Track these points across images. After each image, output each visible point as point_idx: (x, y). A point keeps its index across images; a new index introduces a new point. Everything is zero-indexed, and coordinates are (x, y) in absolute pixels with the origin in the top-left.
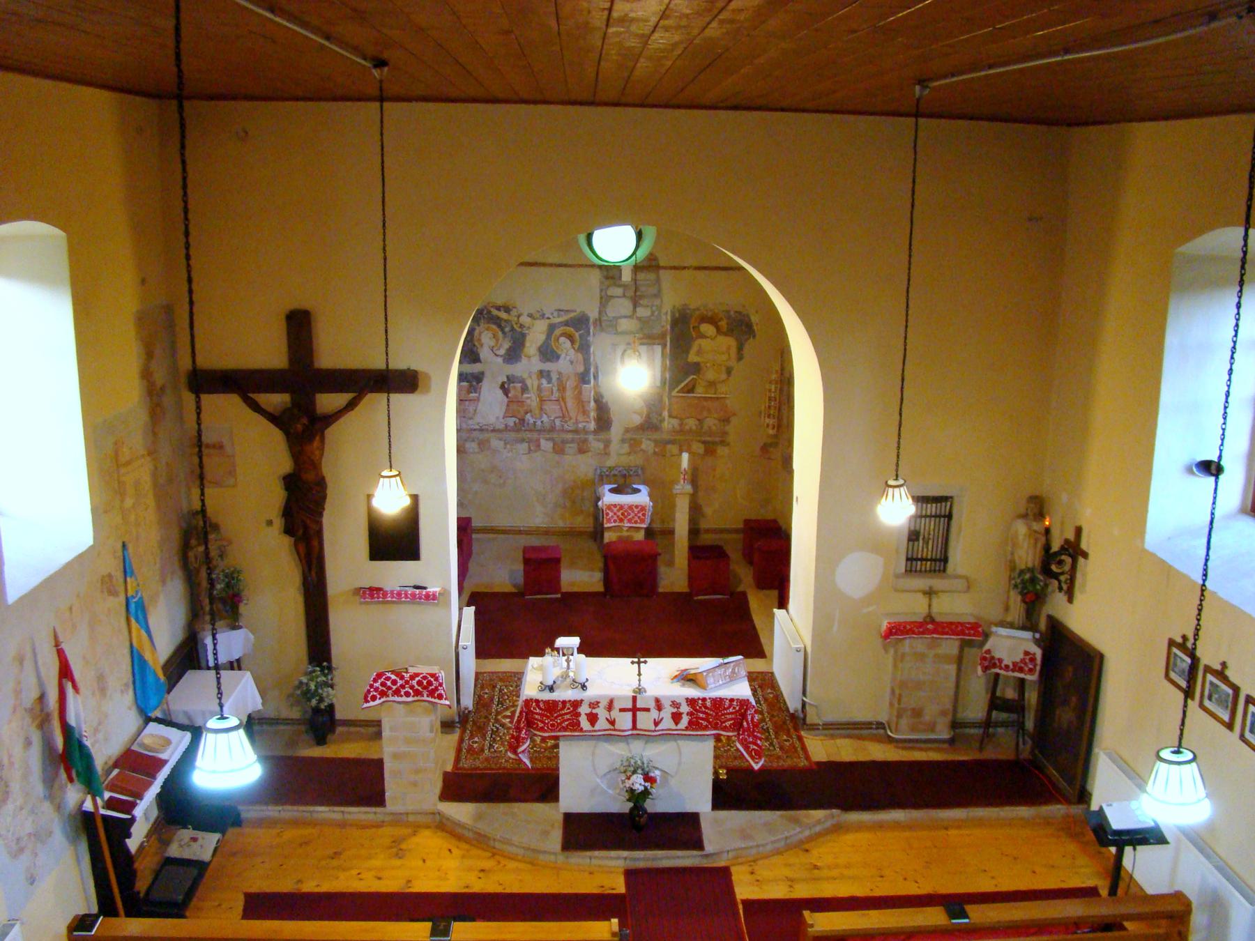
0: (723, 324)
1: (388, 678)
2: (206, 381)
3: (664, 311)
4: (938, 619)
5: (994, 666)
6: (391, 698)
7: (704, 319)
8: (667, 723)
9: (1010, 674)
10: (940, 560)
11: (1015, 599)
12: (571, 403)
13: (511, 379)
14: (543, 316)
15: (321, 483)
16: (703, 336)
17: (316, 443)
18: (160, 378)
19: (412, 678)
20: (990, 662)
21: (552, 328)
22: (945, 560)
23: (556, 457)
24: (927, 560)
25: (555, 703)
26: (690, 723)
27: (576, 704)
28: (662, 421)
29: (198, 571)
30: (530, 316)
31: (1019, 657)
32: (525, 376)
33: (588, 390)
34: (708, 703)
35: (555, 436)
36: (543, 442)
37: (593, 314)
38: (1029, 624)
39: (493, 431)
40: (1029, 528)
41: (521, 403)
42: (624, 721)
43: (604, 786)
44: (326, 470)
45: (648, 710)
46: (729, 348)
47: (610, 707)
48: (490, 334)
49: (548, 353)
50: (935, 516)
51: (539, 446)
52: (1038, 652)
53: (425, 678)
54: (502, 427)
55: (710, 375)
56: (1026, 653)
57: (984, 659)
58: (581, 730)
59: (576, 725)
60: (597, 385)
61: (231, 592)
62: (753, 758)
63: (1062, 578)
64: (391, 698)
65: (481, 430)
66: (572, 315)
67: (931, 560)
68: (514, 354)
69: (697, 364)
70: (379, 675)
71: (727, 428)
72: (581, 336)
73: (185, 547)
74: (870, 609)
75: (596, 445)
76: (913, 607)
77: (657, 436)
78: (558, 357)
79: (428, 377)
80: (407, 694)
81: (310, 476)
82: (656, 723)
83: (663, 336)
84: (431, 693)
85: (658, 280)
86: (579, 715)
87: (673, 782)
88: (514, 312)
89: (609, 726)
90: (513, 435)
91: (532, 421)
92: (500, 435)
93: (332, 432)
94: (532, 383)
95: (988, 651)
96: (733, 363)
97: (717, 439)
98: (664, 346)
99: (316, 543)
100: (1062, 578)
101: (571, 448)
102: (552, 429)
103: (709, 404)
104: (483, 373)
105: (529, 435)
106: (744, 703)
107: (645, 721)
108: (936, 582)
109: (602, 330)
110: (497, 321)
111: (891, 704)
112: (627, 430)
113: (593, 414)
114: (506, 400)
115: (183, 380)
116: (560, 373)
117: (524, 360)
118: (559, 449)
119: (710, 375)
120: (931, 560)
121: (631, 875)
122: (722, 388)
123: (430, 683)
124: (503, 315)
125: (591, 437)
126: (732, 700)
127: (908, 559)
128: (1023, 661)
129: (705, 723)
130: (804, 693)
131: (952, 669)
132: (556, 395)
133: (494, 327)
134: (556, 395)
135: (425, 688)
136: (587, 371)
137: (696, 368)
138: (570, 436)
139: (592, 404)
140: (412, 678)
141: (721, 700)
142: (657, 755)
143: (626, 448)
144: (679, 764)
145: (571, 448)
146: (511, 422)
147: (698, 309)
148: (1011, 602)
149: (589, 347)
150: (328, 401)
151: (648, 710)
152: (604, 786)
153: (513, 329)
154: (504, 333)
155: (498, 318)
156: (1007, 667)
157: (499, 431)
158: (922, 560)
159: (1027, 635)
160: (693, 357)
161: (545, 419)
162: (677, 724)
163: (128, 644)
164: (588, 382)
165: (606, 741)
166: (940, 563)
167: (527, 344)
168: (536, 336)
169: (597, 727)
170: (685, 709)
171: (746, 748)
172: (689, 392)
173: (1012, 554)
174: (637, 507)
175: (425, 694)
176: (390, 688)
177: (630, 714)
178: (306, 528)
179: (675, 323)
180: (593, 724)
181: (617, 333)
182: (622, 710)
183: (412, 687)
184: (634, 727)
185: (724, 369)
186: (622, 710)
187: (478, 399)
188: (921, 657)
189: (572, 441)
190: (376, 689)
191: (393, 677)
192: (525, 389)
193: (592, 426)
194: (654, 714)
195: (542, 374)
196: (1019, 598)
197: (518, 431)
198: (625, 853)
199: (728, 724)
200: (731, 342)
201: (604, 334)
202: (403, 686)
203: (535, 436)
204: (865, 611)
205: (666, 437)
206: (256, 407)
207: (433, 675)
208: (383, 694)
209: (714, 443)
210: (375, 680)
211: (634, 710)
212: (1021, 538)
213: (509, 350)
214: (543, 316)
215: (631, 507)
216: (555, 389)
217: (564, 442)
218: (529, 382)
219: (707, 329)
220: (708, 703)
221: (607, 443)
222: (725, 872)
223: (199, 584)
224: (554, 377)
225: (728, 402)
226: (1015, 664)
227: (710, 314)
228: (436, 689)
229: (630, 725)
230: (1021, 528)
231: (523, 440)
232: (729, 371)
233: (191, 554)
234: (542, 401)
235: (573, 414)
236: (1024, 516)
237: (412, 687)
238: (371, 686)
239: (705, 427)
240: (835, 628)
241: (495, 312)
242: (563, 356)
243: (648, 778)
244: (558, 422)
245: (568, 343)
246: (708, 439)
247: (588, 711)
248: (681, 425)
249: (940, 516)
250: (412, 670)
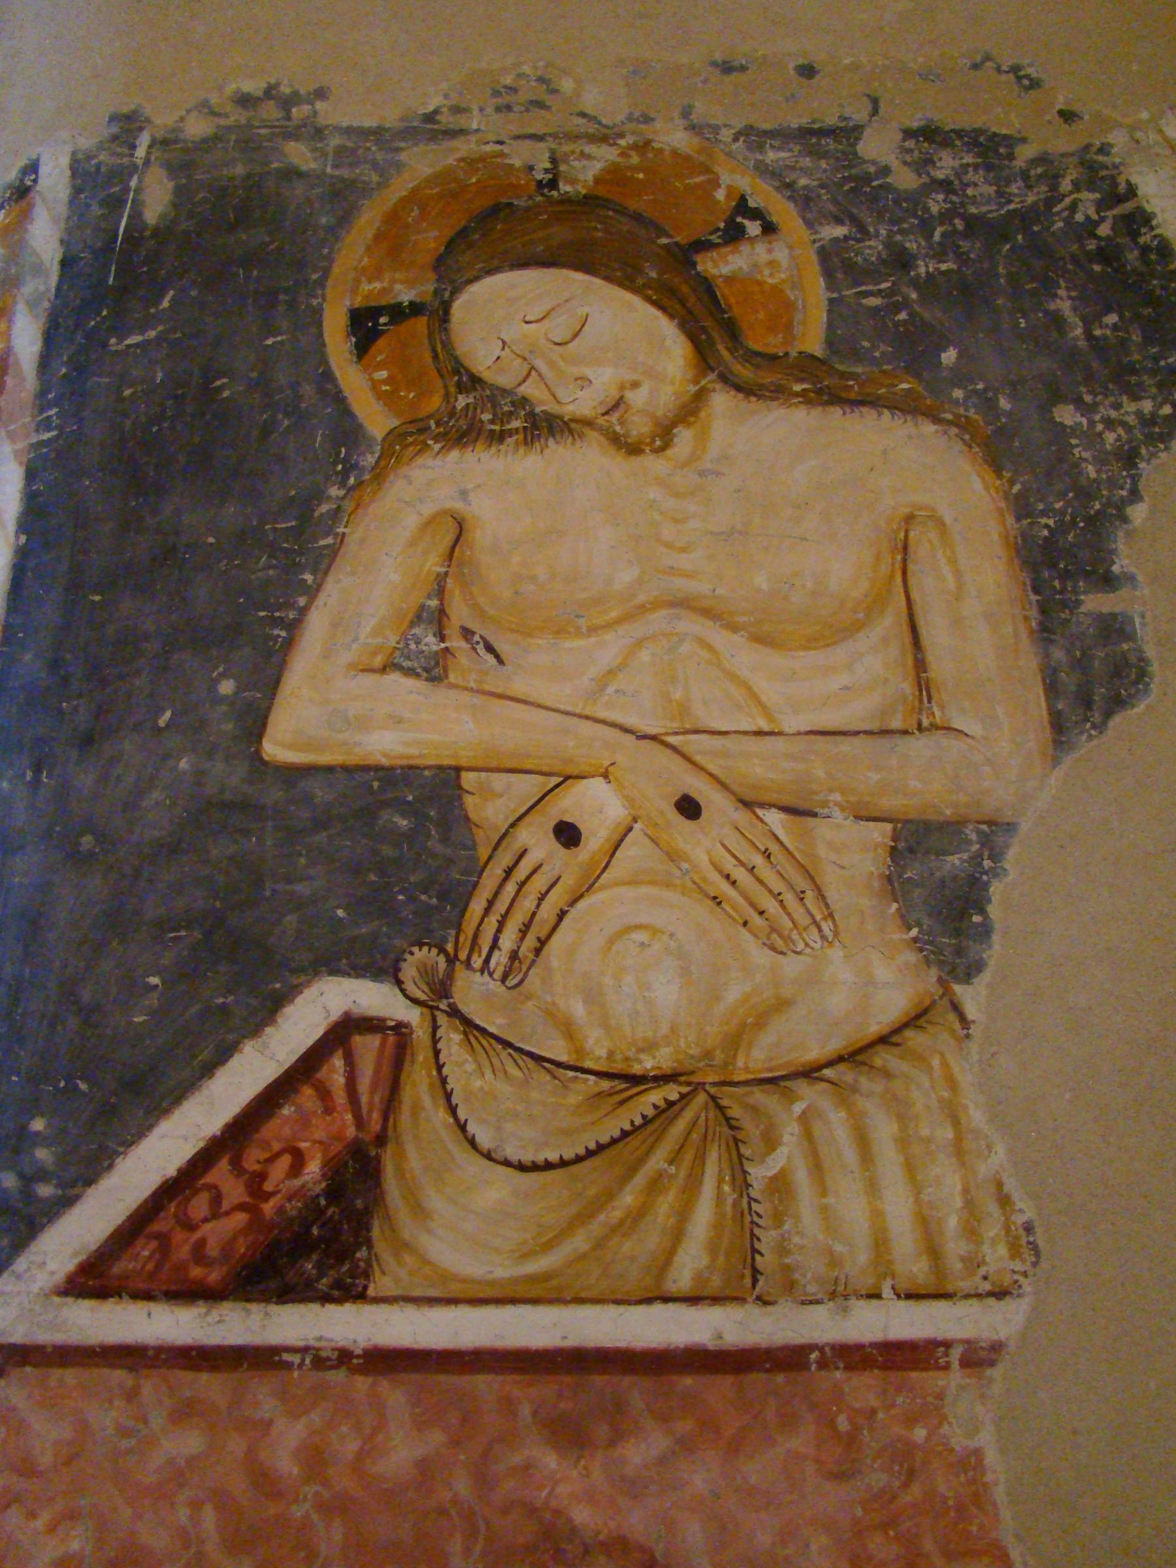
0: (782, 268)
55: (634, 965)
69: (432, 794)
96: (990, 747)
119: (634, 965)
137: (408, 862)
147: (430, 128)
160: (339, 704)
172: (266, 1273)
185: (851, 854)
200: (914, 479)
225: (972, 1417)
227: (586, 170)
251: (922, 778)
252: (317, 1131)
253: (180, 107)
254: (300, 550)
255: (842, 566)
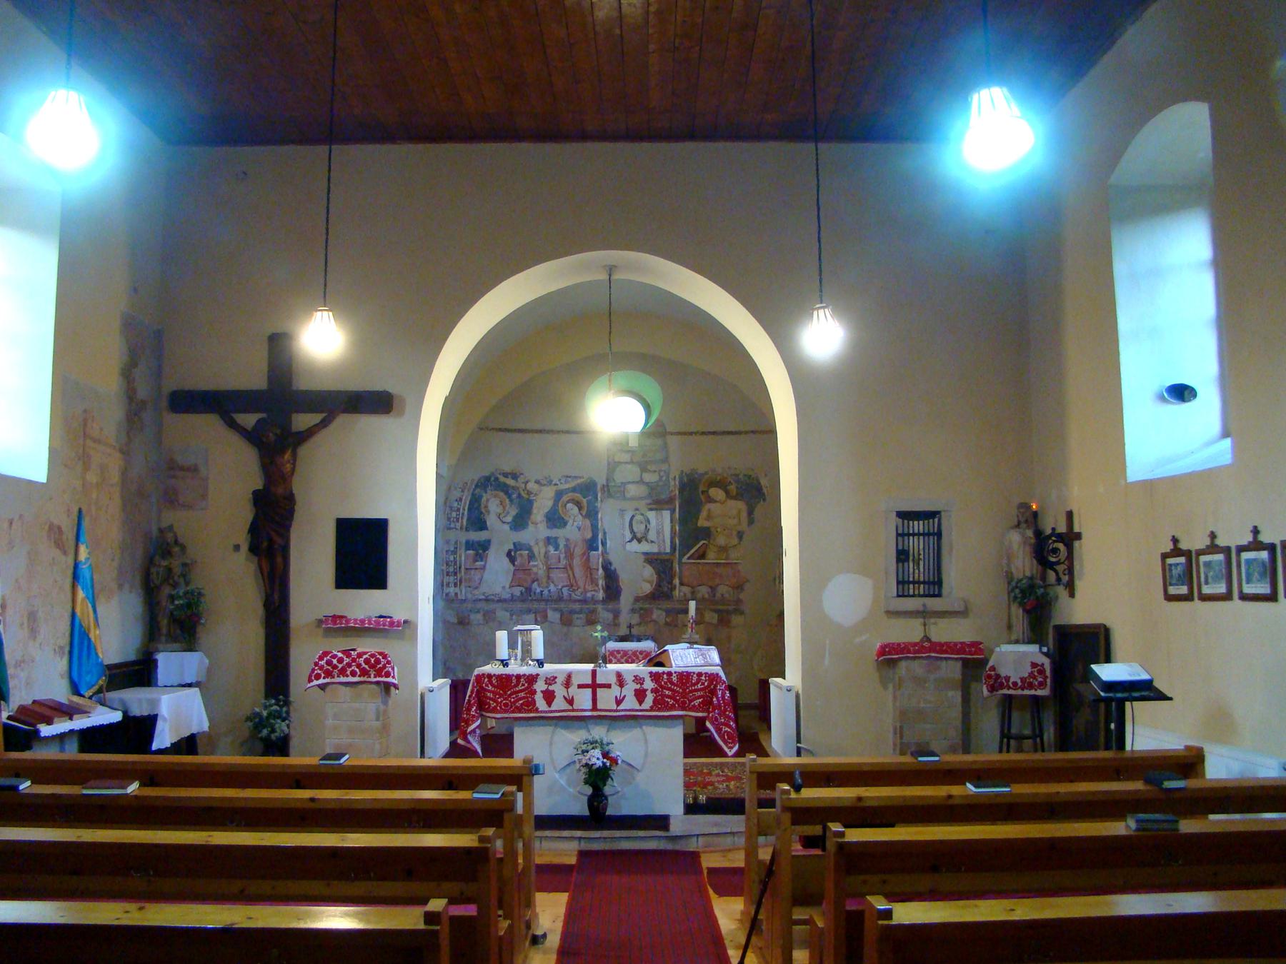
0: (732, 488)
1: (334, 656)
2: (189, 402)
3: (671, 476)
4: (934, 639)
5: (1001, 686)
6: (337, 680)
7: (713, 484)
8: (630, 703)
9: (1019, 692)
10: (934, 583)
11: (1018, 613)
12: (579, 572)
13: (518, 547)
14: (550, 482)
15: (290, 498)
16: (711, 500)
17: (287, 456)
18: (143, 392)
19: (360, 655)
20: (997, 682)
21: (559, 495)
22: (939, 583)
23: (565, 629)
24: (919, 583)
25: (509, 677)
26: (655, 701)
27: (532, 679)
28: (673, 588)
29: (159, 588)
30: (537, 482)
31: (1026, 670)
32: (532, 543)
33: (596, 557)
34: (674, 679)
35: (562, 605)
36: (550, 613)
37: (601, 481)
38: (1036, 636)
39: (499, 601)
40: (1023, 535)
41: (527, 571)
42: (583, 700)
43: (563, 782)
44: (297, 487)
45: (609, 686)
46: (739, 512)
47: (567, 684)
48: (498, 502)
49: (555, 519)
50: (924, 534)
51: (546, 616)
52: (1046, 662)
53: (373, 656)
54: (506, 596)
56: (1034, 665)
57: (989, 677)
58: (537, 710)
59: (530, 705)
60: (605, 553)
61: (189, 612)
62: (725, 742)
63: (1060, 568)
64: (337, 680)
65: (487, 600)
66: (579, 481)
67: (924, 583)
68: (520, 522)
70: (325, 654)
71: (741, 596)
72: (589, 502)
73: (149, 562)
74: (864, 638)
75: (604, 614)
76: (910, 632)
77: (667, 605)
78: (565, 524)
79: (403, 401)
80: (353, 674)
81: (280, 490)
82: (619, 702)
83: (671, 500)
84: (379, 674)
85: (665, 446)
86: (534, 692)
87: (640, 778)
88: (521, 479)
89: (566, 706)
90: (519, 605)
91: (538, 590)
92: (505, 605)
93: (304, 451)
94: (539, 550)
95: (993, 668)
97: (731, 608)
98: (673, 511)
99: (279, 560)
100: (1060, 568)
101: (579, 619)
102: (560, 599)
103: (720, 570)
104: (489, 542)
105: (535, 605)
106: (713, 678)
107: (606, 700)
108: (933, 603)
109: (610, 496)
110: (506, 489)
111: (895, 745)
112: (637, 599)
113: (601, 582)
114: (512, 568)
115: (164, 403)
116: (567, 540)
117: (531, 528)
118: (566, 621)
119: (721, 540)
120: (924, 583)
121: (582, 854)
122: (734, 555)
123: (378, 661)
124: (510, 482)
125: (600, 607)
126: (700, 674)
127: (898, 583)
128: (1031, 675)
129: (671, 702)
130: (799, 741)
131: (956, 696)
132: (563, 562)
133: (502, 494)
134: (563, 562)
135: (372, 666)
136: (595, 537)
137: (707, 533)
138: (577, 606)
139: (601, 571)
140: (360, 655)
141: (688, 674)
142: (624, 743)
143: (635, 619)
144: (646, 755)
145: (579, 619)
146: (517, 591)
147: (706, 473)
148: (1014, 620)
149: (597, 513)
150: (302, 421)
151: (609, 686)
152: (563, 782)
153: (519, 496)
154: (511, 501)
155: (506, 485)
156: (1015, 684)
157: (505, 601)
158: (914, 583)
159: (1033, 648)
160: (702, 523)
161: (552, 587)
162: (641, 702)
163: (70, 610)
164: (597, 549)
165: (566, 728)
166: (935, 586)
167: (535, 511)
168: (543, 503)
169: (554, 707)
170: (649, 684)
171: (719, 730)
172: (699, 558)
173: (1009, 565)
174: (641, 653)
175: (372, 673)
176: (335, 667)
177: (589, 690)
178: (271, 541)
179: (682, 488)
180: (549, 704)
181: (625, 498)
182: (580, 686)
183: (359, 666)
184: (595, 708)
185: (735, 533)
186: (580, 686)
187: (484, 568)
188: (920, 682)
189: (580, 612)
190: (321, 668)
191: (340, 655)
192: (531, 557)
193: (601, 595)
194: (616, 690)
195: (549, 540)
196: (1021, 611)
197: (523, 601)
198: (578, 833)
199: (697, 702)
200: (740, 505)
201: (611, 500)
202: (349, 665)
203: (542, 605)
204: (857, 640)
205: (678, 606)
206: (232, 425)
207: (381, 654)
208: (328, 674)
209: (728, 612)
210: (321, 658)
211: (594, 686)
212: (1015, 547)
213: (516, 517)
214: (550, 482)
215: (635, 653)
216: (562, 556)
217: (572, 612)
218: (536, 550)
219: (717, 493)
220: (674, 679)
221: (616, 614)
222: (695, 856)
223: (158, 603)
224: (562, 544)
226: (1022, 679)
228: (384, 667)
229: (589, 705)
230: (1015, 538)
231: (529, 611)
232: (740, 535)
233: (153, 570)
234: (549, 569)
235: (581, 584)
236: (1018, 526)
237: (359, 666)
238: (316, 664)
239: (718, 595)
240: (827, 662)
241: (502, 479)
242: (571, 522)
243: (605, 755)
244: (565, 591)
245: (576, 509)
246: (720, 607)
247: (544, 687)
248: (693, 593)
249: (929, 534)
250: (359, 650)
251: (739, 528)
252: (701, 552)
253: (687, 470)
254: (699, 511)
255: (735, 512)
